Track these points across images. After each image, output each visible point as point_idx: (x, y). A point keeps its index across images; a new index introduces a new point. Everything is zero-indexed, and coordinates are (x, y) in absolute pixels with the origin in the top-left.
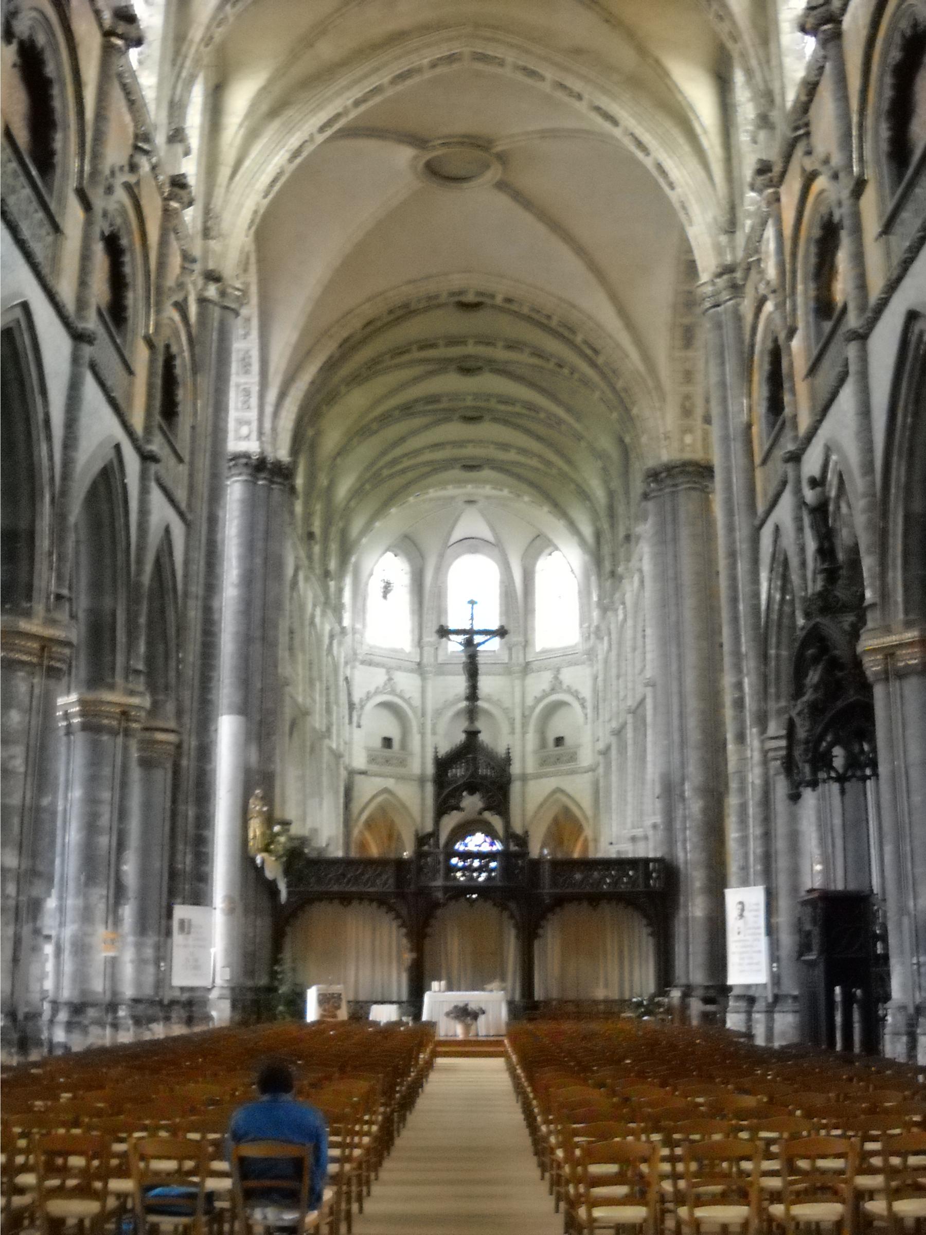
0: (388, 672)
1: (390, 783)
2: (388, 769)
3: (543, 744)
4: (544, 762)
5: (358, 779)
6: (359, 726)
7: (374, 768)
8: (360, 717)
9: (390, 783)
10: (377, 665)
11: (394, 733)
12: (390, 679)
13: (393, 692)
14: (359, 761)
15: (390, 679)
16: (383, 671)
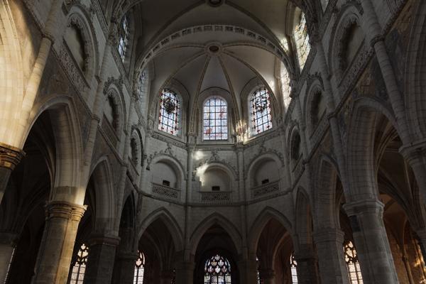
0: (168, 145)
1: (166, 205)
2: (165, 197)
3: (256, 183)
4: (257, 193)
5: (144, 198)
6: (148, 169)
7: (156, 194)
8: (149, 164)
9: (166, 205)
10: (162, 139)
11: (171, 177)
12: (169, 148)
13: (171, 155)
14: (147, 189)
15: (169, 148)
16: (166, 144)
